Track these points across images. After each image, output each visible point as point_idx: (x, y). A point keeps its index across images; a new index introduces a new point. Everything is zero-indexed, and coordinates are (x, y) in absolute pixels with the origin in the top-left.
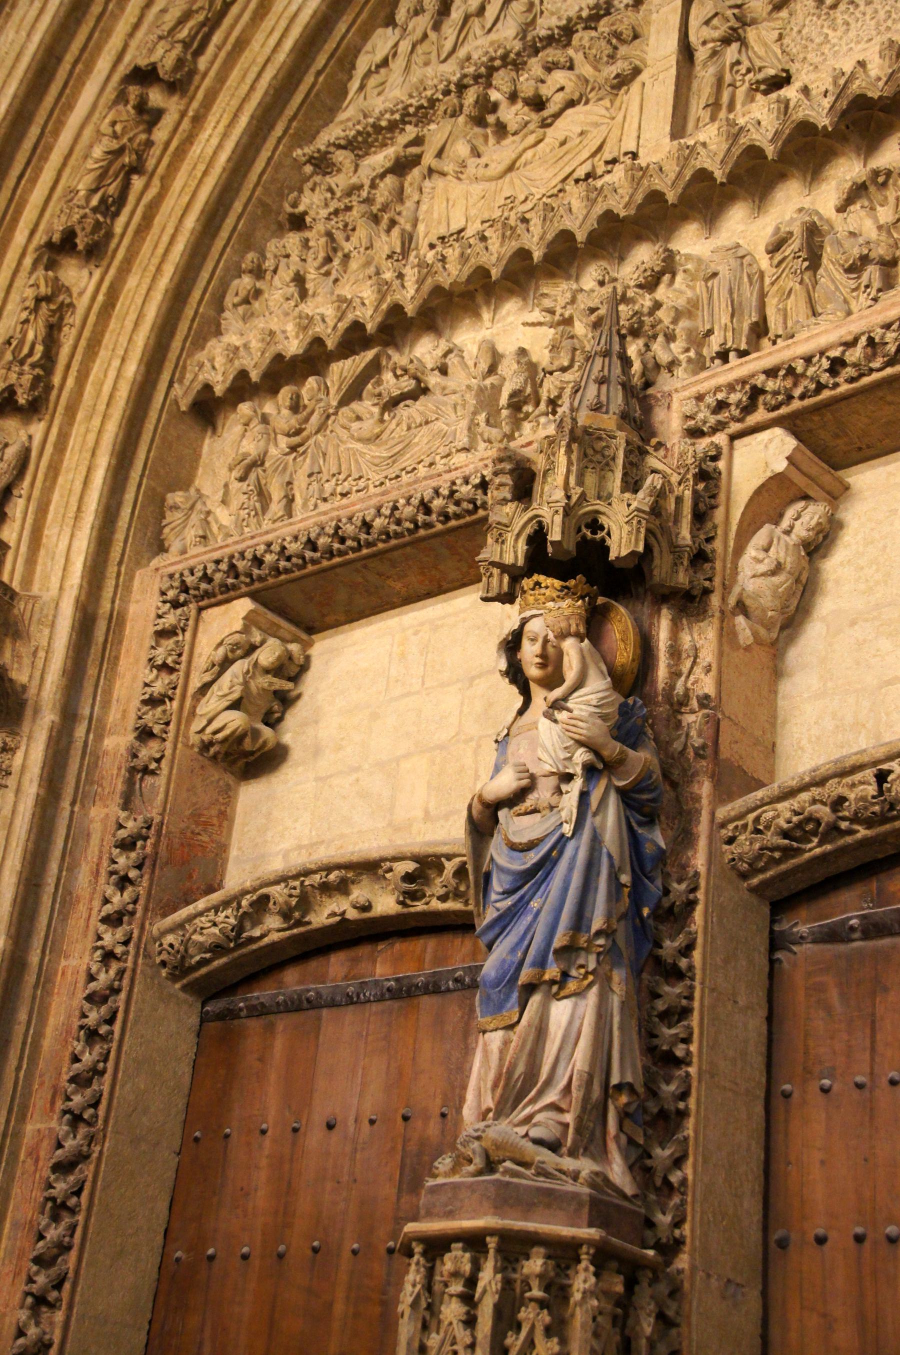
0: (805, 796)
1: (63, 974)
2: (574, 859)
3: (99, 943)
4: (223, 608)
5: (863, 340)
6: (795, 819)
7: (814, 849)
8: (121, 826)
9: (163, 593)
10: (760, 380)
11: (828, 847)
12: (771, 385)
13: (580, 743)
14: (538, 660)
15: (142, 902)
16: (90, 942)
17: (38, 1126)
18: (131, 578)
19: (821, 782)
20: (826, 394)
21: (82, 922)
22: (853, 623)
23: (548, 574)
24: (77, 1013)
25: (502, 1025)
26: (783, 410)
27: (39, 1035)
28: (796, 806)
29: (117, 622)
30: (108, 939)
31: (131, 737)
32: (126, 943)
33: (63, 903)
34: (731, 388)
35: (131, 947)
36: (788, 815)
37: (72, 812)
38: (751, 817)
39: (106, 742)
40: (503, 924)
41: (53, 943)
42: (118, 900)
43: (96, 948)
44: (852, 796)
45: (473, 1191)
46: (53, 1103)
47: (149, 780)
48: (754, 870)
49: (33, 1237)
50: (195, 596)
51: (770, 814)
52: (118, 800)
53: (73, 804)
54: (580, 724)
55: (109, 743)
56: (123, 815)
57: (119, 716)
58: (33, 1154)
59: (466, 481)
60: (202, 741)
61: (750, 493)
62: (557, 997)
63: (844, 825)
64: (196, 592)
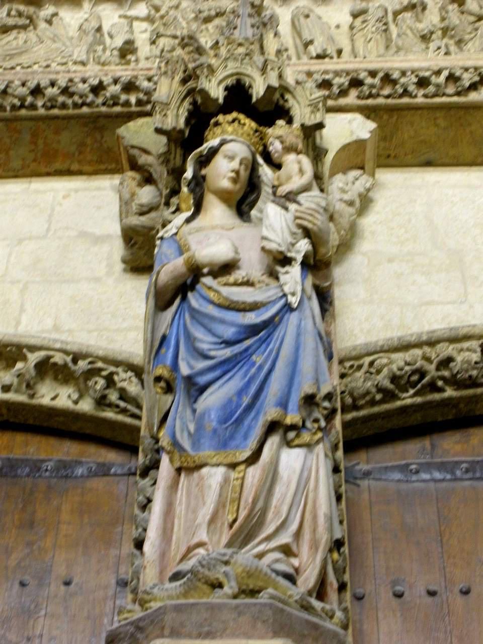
0: (418, 352)
2: (279, 335)
5: (445, 73)
6: (407, 368)
7: (408, 399)
10: (362, 75)
11: (419, 400)
12: (369, 80)
13: (307, 233)
14: (233, 175)
19: (432, 343)
20: (406, 100)
22: (390, 260)
23: (249, 115)
25: (230, 460)
26: (370, 102)
28: (408, 359)
34: (337, 74)
36: (402, 364)
38: (367, 360)
40: (225, 368)
44: (459, 359)
45: (240, 614)
48: (355, 407)
51: (385, 361)
54: (317, 215)
59: (84, 81)
61: (338, 148)
62: (289, 444)
63: (440, 383)
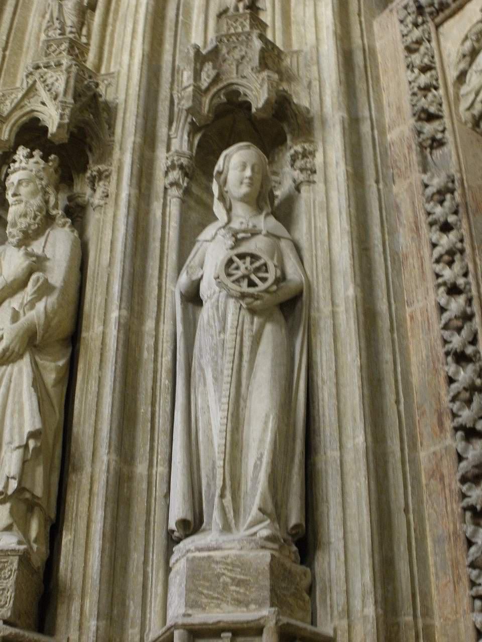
1: (412, 318)
3: (440, 280)
4: (457, 17)
8: (426, 186)
9: (402, 22)
15: (467, 240)
16: (431, 282)
17: (432, 449)
18: (370, 26)
21: (417, 272)
24: (439, 342)
27: (406, 374)
29: (370, 53)
30: (448, 274)
31: (412, 121)
32: (466, 275)
33: (393, 262)
35: (471, 277)
37: (379, 190)
39: (389, 137)
41: (395, 294)
42: (446, 241)
43: (439, 286)
46: (441, 424)
47: (438, 153)
49: (462, 544)
50: (431, 14)
52: (416, 168)
53: (377, 182)
55: (391, 136)
56: (425, 178)
57: (394, 113)
58: (436, 474)
60: (474, 116)
64: (433, 9)
